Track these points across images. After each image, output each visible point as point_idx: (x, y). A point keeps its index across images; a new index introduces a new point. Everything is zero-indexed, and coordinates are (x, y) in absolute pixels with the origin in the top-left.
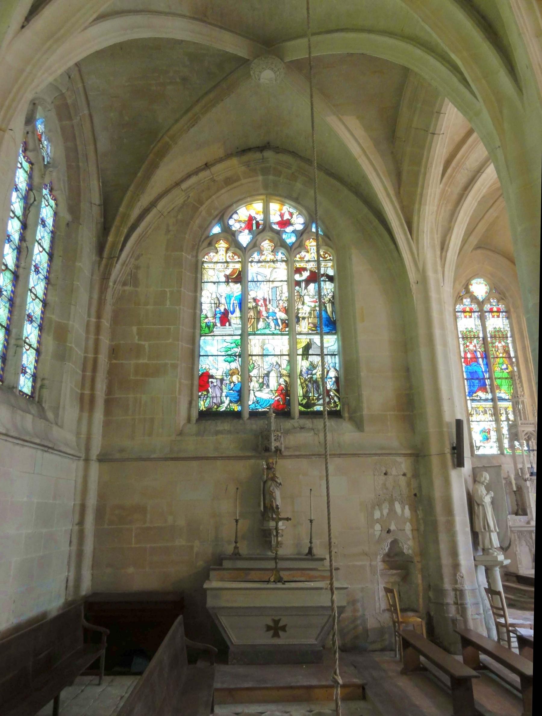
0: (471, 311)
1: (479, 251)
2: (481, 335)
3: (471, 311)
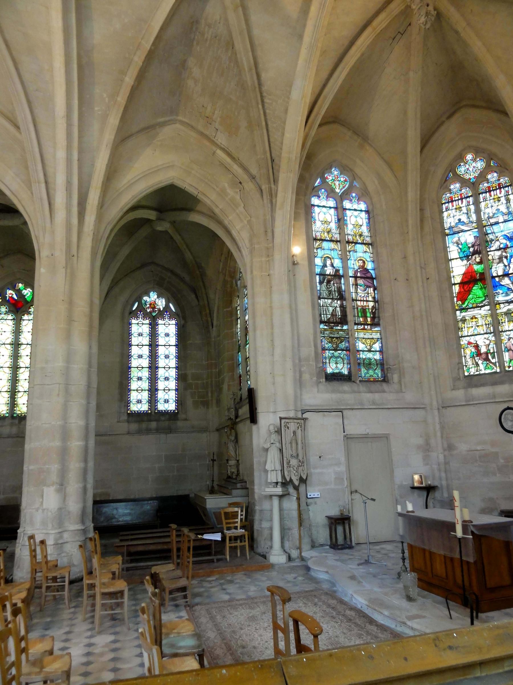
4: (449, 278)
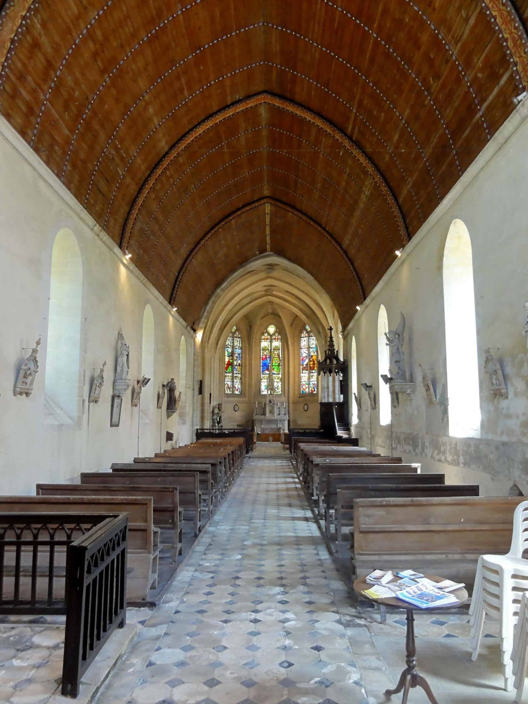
3: (267, 339)
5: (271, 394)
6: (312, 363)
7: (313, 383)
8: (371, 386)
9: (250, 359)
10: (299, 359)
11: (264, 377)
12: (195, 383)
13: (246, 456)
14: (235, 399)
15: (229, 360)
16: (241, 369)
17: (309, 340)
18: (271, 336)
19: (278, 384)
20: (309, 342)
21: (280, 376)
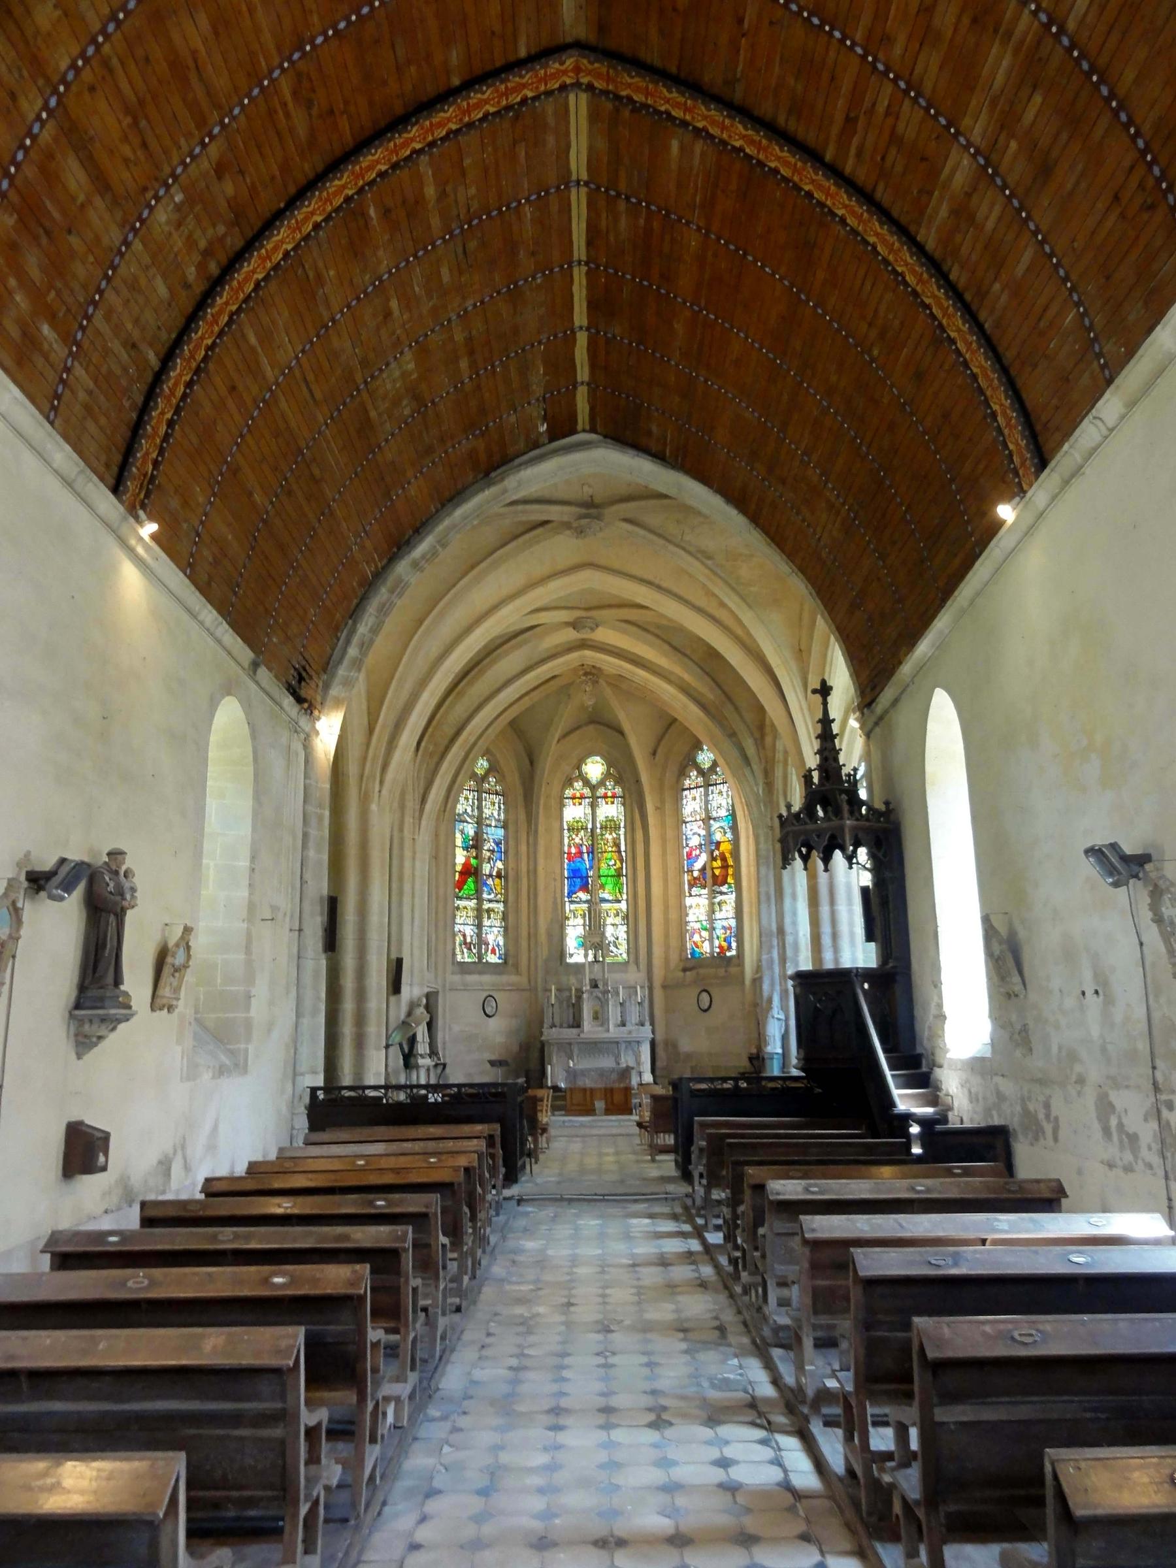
0: (582, 797)
1: (591, 727)
2: (590, 826)
3: (582, 797)
4: (454, 865)
5: (596, 961)
6: (718, 863)
7: (725, 923)
8: (1142, 860)
9: (532, 856)
10: (680, 855)
11: (573, 912)
12: (307, 906)
13: (507, 1193)
14: (486, 978)
15: (468, 858)
16: (506, 888)
17: (706, 795)
18: (593, 788)
19: (616, 931)
20: (707, 802)
21: (623, 906)
